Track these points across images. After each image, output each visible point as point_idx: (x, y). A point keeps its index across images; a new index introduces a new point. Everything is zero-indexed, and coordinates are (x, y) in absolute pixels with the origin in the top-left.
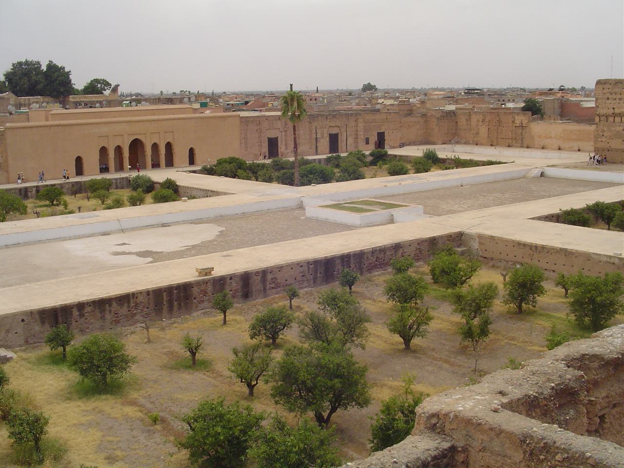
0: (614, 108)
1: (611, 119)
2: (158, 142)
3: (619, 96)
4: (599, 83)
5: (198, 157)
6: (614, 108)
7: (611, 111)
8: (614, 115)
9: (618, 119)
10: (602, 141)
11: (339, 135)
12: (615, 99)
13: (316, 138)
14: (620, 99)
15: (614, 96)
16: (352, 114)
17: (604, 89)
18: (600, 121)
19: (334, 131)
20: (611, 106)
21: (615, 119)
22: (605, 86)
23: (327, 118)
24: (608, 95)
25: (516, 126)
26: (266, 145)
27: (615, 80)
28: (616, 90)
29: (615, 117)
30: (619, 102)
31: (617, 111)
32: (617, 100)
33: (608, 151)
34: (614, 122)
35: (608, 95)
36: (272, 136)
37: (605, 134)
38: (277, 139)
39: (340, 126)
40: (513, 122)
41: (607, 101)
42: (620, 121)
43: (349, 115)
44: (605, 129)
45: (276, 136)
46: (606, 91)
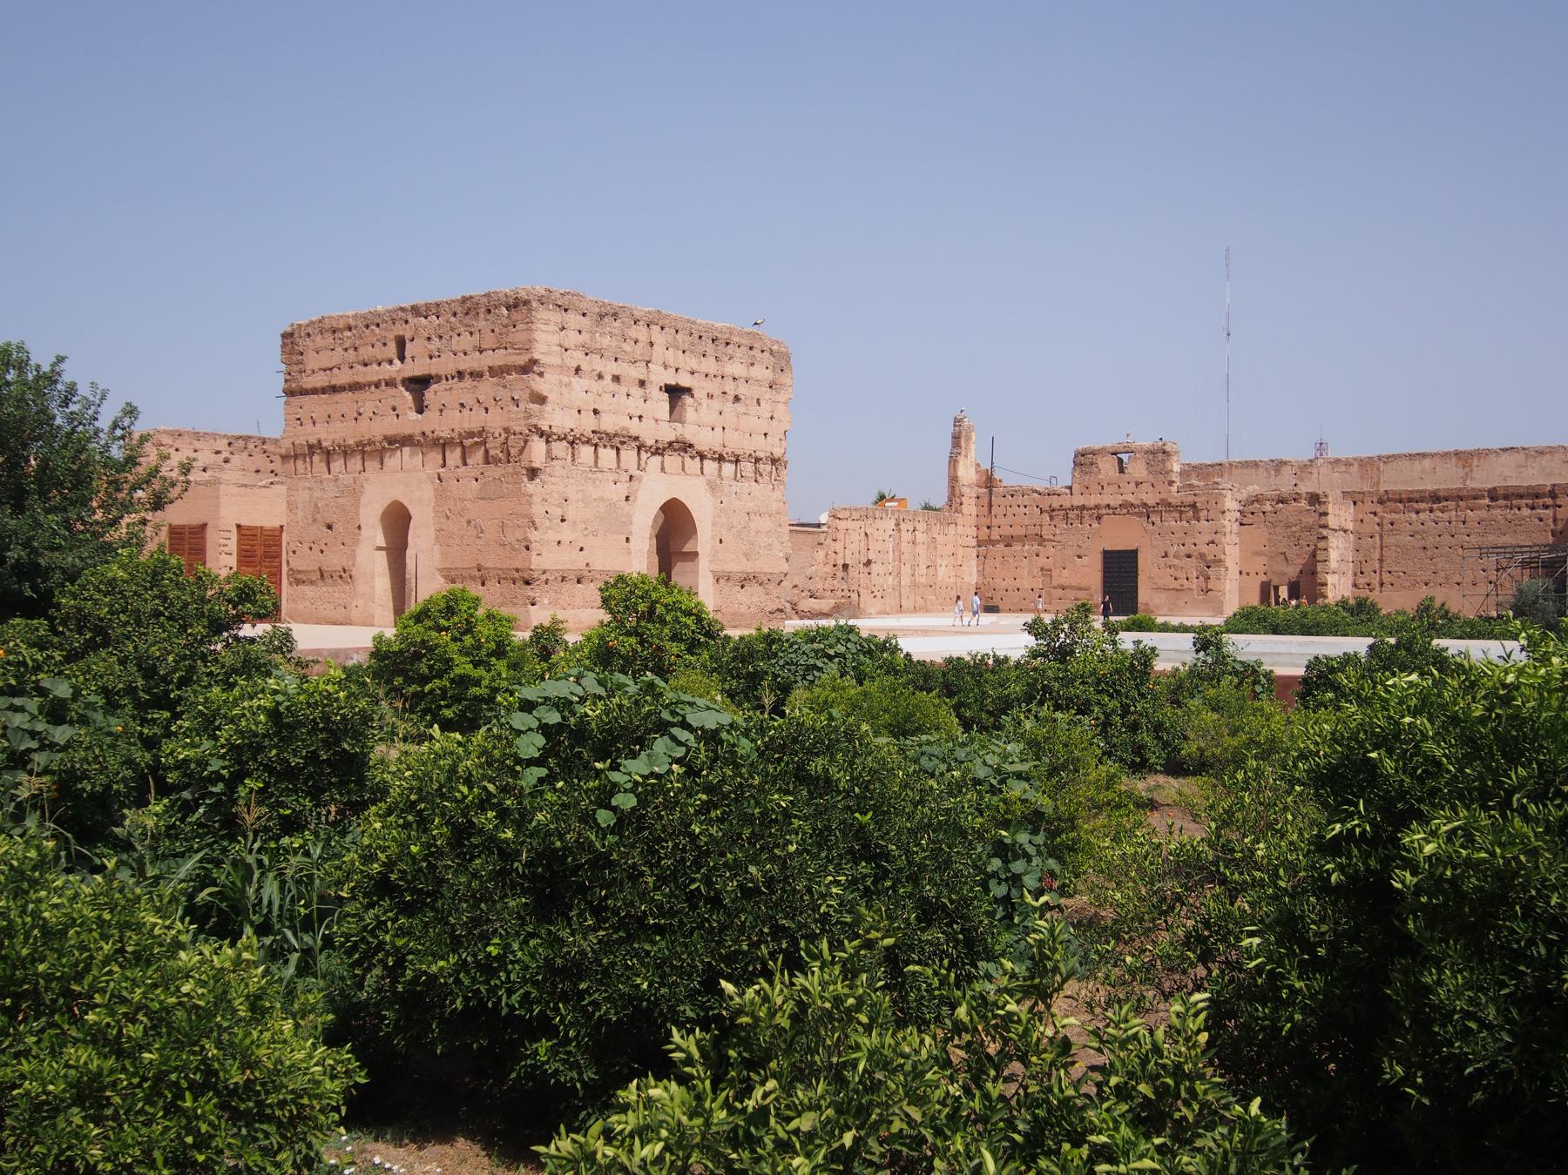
0: (596, 412)
3: (611, 368)
6: (596, 412)
7: (587, 424)
8: (600, 439)
9: (607, 455)
12: (600, 377)
14: (616, 379)
15: (598, 364)
20: (590, 402)
21: (601, 450)
24: (576, 358)
28: (606, 342)
30: (614, 386)
31: (609, 423)
32: (608, 378)
35: (576, 358)
42: (614, 466)
44: (572, 493)
46: (572, 338)
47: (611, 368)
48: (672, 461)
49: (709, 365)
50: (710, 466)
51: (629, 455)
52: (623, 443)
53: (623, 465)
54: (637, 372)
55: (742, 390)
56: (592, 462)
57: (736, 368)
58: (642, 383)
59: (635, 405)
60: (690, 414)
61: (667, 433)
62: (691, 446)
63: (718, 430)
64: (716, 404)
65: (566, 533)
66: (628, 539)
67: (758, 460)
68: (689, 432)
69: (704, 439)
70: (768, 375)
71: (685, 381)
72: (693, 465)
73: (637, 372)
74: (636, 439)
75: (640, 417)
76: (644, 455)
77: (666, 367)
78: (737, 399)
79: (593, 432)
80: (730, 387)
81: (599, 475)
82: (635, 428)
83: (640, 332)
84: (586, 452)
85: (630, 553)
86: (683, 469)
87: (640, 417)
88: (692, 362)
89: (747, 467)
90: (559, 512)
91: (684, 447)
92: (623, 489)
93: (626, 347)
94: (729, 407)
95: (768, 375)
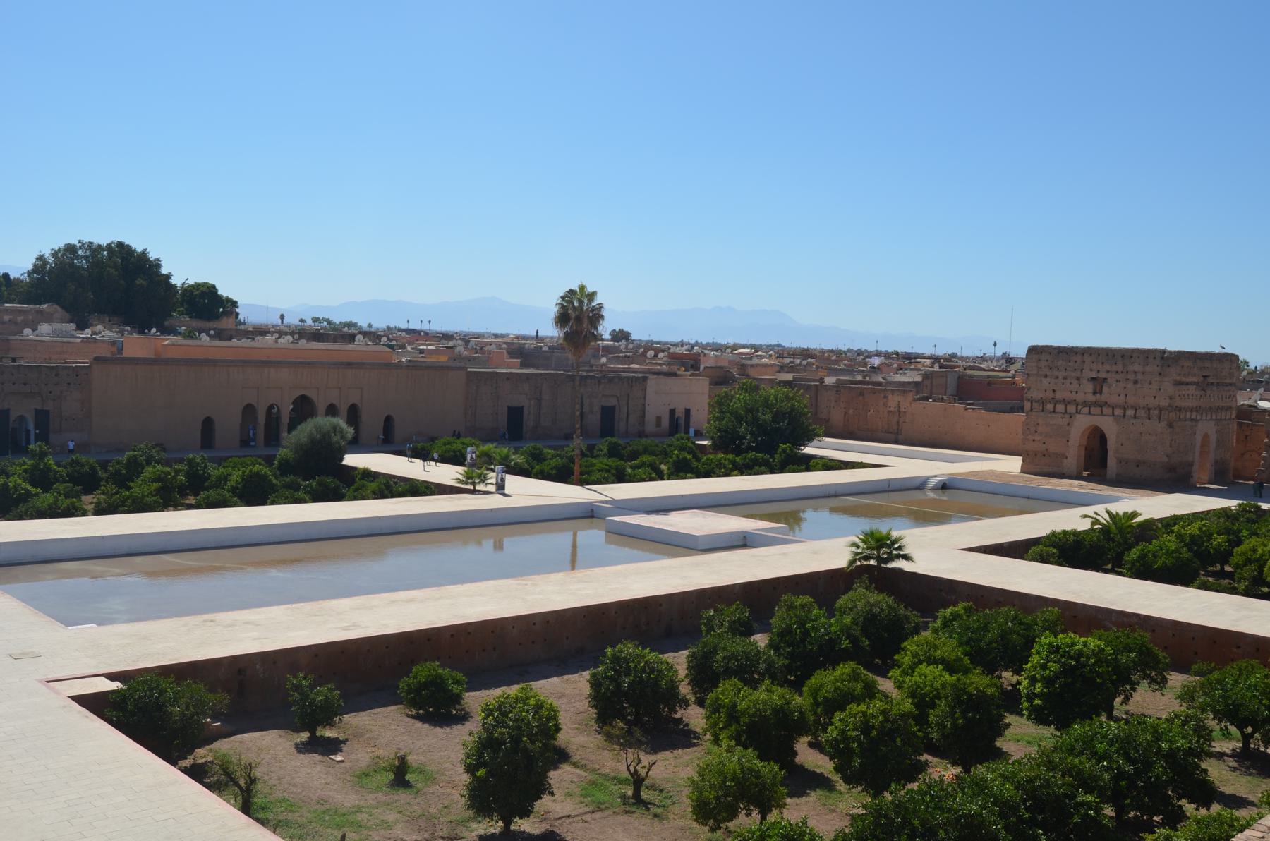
1: (1050, 407)
2: (335, 402)
4: (1033, 350)
5: (399, 432)
6: (1054, 391)
7: (1051, 395)
8: (1055, 402)
9: (1060, 408)
10: (1034, 440)
11: (617, 408)
13: (582, 414)
15: (1056, 373)
16: (637, 378)
17: (1039, 360)
18: (1032, 409)
19: (612, 402)
21: (1057, 406)
22: (1044, 357)
23: (599, 382)
25: (889, 412)
26: (503, 419)
27: (1059, 347)
29: (1055, 404)
30: (1062, 381)
31: (1059, 395)
32: (1060, 378)
33: (1044, 455)
34: (1054, 412)
36: (515, 404)
37: (1040, 429)
38: (522, 407)
39: (619, 396)
40: (885, 405)
41: (1043, 379)
42: (1063, 411)
43: (634, 379)
45: (521, 405)
46: (1043, 363)
47: (1061, 374)
48: (1095, 410)
49: (1120, 367)
50: (1118, 412)
51: (1072, 409)
52: (1069, 403)
53: (1068, 411)
54: (1074, 374)
55: (1139, 377)
56: (1052, 410)
57: (1137, 367)
58: (1078, 379)
59: (1075, 386)
60: (1105, 389)
61: (1091, 398)
62: (1106, 403)
63: (1122, 397)
64: (1122, 384)
65: (1037, 438)
66: (1068, 441)
67: (1149, 409)
68: (1103, 398)
69: (1114, 399)
70: (1159, 369)
71: (1103, 375)
72: (1109, 411)
73: (1078, 374)
74: (1075, 400)
75: (1077, 392)
76: (1079, 407)
77: (1091, 370)
78: (1136, 382)
79: (1053, 398)
80: (1131, 377)
81: (1054, 415)
82: (1073, 396)
83: (1079, 358)
84: (1050, 407)
85: (1068, 446)
86: (1102, 412)
87: (1077, 392)
88: (1108, 367)
89: (1142, 413)
90: (1034, 428)
91: (1101, 405)
92: (1066, 421)
93: (1070, 364)
94: (1130, 385)
95: (1159, 369)
